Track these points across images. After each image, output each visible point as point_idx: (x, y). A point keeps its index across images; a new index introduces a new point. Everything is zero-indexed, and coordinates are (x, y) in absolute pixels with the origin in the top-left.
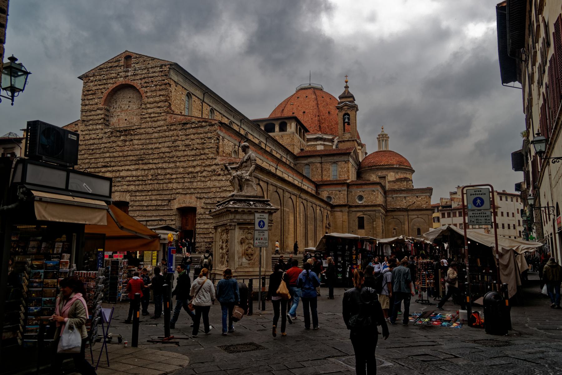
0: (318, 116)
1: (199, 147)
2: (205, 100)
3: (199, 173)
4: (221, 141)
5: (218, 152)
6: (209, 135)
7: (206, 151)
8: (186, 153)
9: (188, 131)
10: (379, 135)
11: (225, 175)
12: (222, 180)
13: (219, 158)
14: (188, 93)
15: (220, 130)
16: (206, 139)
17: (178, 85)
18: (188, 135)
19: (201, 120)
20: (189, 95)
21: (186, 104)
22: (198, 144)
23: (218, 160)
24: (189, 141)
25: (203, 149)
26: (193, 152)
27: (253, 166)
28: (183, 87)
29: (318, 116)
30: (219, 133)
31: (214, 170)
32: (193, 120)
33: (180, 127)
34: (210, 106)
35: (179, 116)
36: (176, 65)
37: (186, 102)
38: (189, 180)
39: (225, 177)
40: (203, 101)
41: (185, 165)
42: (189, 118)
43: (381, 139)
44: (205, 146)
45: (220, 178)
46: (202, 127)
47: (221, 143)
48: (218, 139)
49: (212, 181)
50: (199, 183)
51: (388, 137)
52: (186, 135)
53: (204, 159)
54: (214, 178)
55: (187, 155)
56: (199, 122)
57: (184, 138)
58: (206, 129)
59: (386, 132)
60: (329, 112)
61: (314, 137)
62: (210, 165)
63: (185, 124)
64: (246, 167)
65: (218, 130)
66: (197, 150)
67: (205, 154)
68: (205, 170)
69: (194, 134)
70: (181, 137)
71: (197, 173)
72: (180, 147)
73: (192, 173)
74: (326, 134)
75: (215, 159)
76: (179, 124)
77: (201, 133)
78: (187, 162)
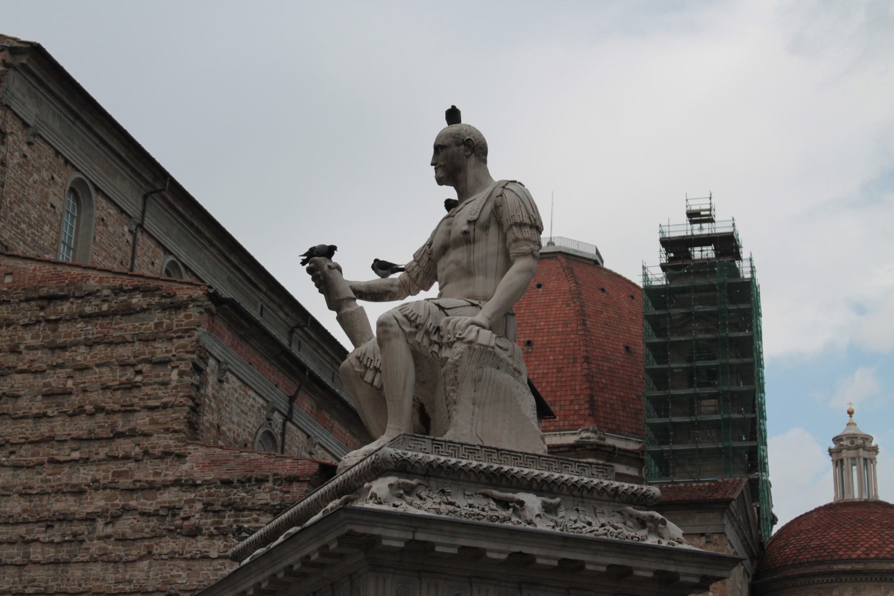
0: (587, 359)
1: (109, 400)
2: (149, 224)
3: (100, 523)
4: (212, 379)
5: (193, 427)
6: (161, 349)
7: (141, 420)
8: (44, 428)
9: (62, 328)
10: (837, 440)
11: (223, 533)
12: (205, 557)
13: (197, 453)
14: (80, 182)
15: (211, 329)
16: (146, 368)
17: (38, 143)
18: (63, 348)
19: (128, 283)
20: (80, 191)
21: (65, 230)
22: (105, 388)
23: (195, 463)
24: (62, 373)
25: (128, 411)
26: (83, 425)
27: (519, 264)
28: (57, 153)
29: (587, 359)
30: (208, 342)
31: (173, 510)
32: (92, 284)
33: (30, 311)
34: (167, 251)
35: (31, 266)
36: (37, 51)
37: (67, 219)
38: (51, 552)
39: (219, 543)
40: (140, 226)
41: (36, 480)
42: (75, 271)
43: (845, 454)
44: (135, 398)
45: (201, 543)
46: (128, 311)
47: (210, 390)
48: (198, 369)
49: (160, 558)
50: (96, 569)
51: (875, 450)
52: (54, 348)
53: (127, 457)
54: (168, 545)
55: (49, 439)
56: (118, 291)
57: (43, 358)
58: (149, 324)
59: (863, 429)
60: (627, 348)
61: (571, 439)
62: (152, 488)
63: (51, 299)
64: (468, 272)
65: (203, 329)
66: (100, 417)
67: (132, 433)
68: (126, 510)
69: (90, 344)
70: (28, 356)
71: (90, 519)
72: (23, 403)
73: (65, 518)
74: (616, 431)
75: (181, 457)
76: (28, 300)
77: (124, 342)
78: (48, 468)
